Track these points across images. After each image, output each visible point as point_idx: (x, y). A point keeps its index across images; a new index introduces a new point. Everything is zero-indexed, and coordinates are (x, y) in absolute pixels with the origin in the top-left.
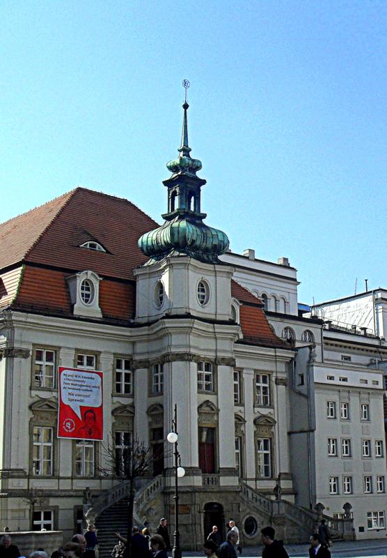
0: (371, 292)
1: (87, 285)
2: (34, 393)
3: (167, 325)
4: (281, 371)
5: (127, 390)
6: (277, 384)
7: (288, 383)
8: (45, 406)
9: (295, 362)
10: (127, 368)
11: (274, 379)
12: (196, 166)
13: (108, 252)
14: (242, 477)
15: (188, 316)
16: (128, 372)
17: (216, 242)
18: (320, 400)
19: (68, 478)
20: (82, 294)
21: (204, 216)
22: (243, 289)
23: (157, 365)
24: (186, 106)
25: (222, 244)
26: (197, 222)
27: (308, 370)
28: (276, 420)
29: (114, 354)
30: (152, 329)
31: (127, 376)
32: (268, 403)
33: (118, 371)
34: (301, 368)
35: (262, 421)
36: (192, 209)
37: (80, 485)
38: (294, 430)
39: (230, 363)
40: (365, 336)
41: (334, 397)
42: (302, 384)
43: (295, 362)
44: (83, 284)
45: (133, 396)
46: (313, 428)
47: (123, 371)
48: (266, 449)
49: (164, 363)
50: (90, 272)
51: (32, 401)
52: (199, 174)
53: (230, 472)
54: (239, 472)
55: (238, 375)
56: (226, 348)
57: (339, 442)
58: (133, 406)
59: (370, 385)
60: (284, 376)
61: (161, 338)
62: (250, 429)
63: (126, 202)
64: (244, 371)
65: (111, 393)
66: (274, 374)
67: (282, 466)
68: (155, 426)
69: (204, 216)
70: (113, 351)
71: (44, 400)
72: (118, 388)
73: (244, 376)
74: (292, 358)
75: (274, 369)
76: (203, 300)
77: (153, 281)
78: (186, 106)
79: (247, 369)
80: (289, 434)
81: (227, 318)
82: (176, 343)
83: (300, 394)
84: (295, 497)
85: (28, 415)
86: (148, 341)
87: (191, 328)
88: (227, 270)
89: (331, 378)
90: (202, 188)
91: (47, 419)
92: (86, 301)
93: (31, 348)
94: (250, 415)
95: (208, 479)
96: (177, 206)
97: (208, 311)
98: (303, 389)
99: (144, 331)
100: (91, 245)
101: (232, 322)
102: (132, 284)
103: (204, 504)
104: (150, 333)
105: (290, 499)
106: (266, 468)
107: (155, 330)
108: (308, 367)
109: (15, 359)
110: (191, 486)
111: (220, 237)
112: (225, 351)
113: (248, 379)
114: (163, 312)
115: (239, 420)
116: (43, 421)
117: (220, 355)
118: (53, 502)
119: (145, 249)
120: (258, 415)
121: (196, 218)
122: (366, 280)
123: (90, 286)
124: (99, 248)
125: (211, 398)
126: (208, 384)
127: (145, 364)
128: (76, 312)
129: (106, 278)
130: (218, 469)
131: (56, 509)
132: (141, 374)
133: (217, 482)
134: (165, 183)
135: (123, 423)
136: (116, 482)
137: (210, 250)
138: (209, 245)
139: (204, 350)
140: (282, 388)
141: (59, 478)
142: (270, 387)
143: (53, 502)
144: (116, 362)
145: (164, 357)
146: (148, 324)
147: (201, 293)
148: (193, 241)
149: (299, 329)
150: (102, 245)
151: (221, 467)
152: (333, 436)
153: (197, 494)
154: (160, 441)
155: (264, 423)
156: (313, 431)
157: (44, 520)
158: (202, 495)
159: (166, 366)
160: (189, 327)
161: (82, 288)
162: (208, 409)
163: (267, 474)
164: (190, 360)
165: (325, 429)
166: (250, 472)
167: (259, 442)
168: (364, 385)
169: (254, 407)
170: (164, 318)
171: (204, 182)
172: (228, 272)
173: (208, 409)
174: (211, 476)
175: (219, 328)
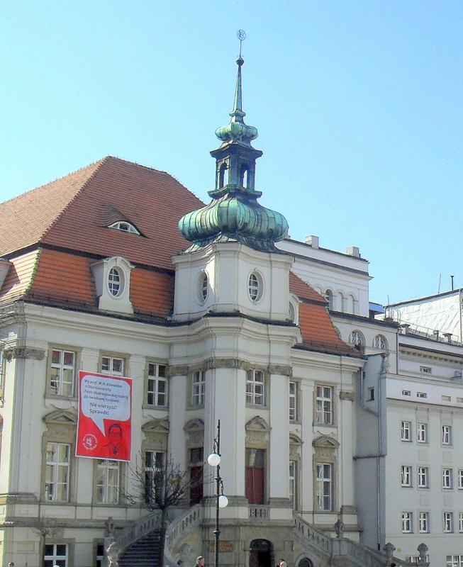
1: (116, 274)
2: (49, 402)
3: (211, 325)
4: (346, 382)
5: (161, 401)
8: (62, 418)
9: (364, 373)
10: (161, 374)
13: (142, 235)
14: (296, 509)
15: (237, 314)
16: (162, 379)
17: (272, 226)
18: (393, 419)
19: (87, 506)
20: (110, 284)
21: (260, 194)
22: (304, 283)
23: (199, 373)
24: (240, 62)
25: (280, 230)
26: (250, 201)
28: (339, 441)
29: (146, 357)
30: (193, 329)
31: (162, 385)
32: (330, 420)
33: (151, 378)
34: (371, 381)
35: (322, 443)
36: (245, 185)
37: (102, 514)
38: (361, 455)
39: (286, 372)
40: (450, 343)
41: (410, 416)
42: (373, 399)
43: (364, 373)
44: (111, 272)
45: (168, 409)
46: (384, 454)
47: (157, 378)
48: (326, 476)
49: (206, 370)
50: (120, 258)
51: (46, 411)
52: (255, 144)
53: (283, 503)
54: (293, 502)
55: (294, 386)
56: (281, 353)
57: (415, 470)
58: (167, 421)
60: (349, 389)
61: (203, 340)
62: (307, 452)
63: (165, 177)
64: (303, 382)
65: (141, 404)
66: (339, 387)
67: (345, 495)
68: (194, 446)
69: (260, 194)
70: (145, 355)
71: (61, 410)
72: (150, 400)
74: (360, 368)
75: (338, 380)
78: (240, 62)
79: (305, 379)
80: (355, 459)
81: (283, 318)
82: (222, 346)
83: (369, 411)
84: (360, 535)
86: (188, 343)
87: (240, 329)
88: (285, 260)
89: (407, 393)
90: (257, 160)
91: (63, 434)
92: (115, 293)
93: (46, 347)
94: (308, 434)
95: (256, 510)
96: (226, 182)
97: (261, 309)
98: (373, 405)
99: (183, 330)
100: (122, 226)
101: (289, 323)
102: (172, 274)
103: (250, 541)
104: (190, 333)
105: (354, 537)
106: (326, 500)
107: (197, 330)
108: (380, 379)
110: (235, 519)
111: (278, 221)
112: (279, 357)
113: (307, 392)
114: (207, 308)
115: (295, 441)
117: (274, 362)
118: (68, 534)
119: (187, 233)
120: (319, 435)
121: (248, 197)
122: (452, 277)
123: (119, 276)
124: (131, 230)
125: (262, 413)
126: (259, 396)
127: (184, 371)
129: (139, 266)
130: (268, 500)
131: (72, 542)
132: (179, 385)
133: (266, 514)
134: (214, 154)
135: (154, 441)
136: (145, 512)
137: (265, 237)
138: (264, 230)
139: (256, 355)
141: (76, 505)
142: (333, 402)
143: (68, 534)
144: (148, 368)
145: (207, 362)
146: (189, 323)
147: (254, 288)
148: (246, 224)
149: (370, 333)
150: (135, 227)
151: (271, 496)
152: (407, 464)
154: (199, 464)
155: (325, 445)
156: (383, 456)
157: (58, 554)
159: (208, 373)
160: (237, 328)
161: (110, 278)
162: (257, 426)
163: (326, 507)
164: (238, 368)
165: (398, 453)
166: (307, 502)
167: (318, 468)
168: (447, 403)
169: (313, 425)
170: (207, 315)
171: (259, 154)
172: (286, 263)
173: (257, 426)
174: (259, 507)
175: (274, 330)
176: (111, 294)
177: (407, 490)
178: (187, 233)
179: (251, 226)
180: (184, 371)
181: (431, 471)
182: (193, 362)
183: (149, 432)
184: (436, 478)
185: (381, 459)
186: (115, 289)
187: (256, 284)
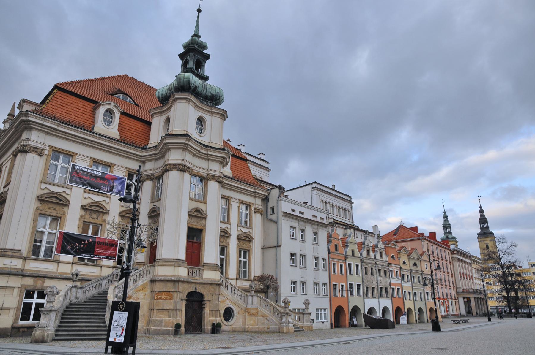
0: (308, 184)
1: (110, 112)
2: (44, 186)
6: (255, 212)
7: (263, 213)
9: (268, 199)
11: (253, 209)
13: (136, 104)
14: (226, 276)
17: (213, 92)
18: (285, 225)
19: (68, 263)
20: (105, 120)
23: (158, 178)
24: (199, 11)
27: (278, 203)
28: (253, 237)
29: (127, 168)
32: (248, 223)
34: (272, 203)
41: (295, 224)
42: (273, 212)
48: (245, 257)
50: (112, 104)
53: (211, 267)
57: (298, 256)
59: (318, 220)
61: (163, 156)
64: (232, 200)
66: (254, 206)
71: (53, 193)
73: (232, 203)
74: (266, 196)
75: (253, 202)
76: (201, 131)
77: (164, 117)
78: (199, 11)
80: (264, 248)
83: (271, 220)
85: (34, 204)
87: (188, 145)
89: (293, 211)
91: (55, 209)
93: (47, 148)
97: (205, 139)
98: (274, 217)
103: (187, 292)
106: (245, 272)
108: (278, 201)
109: (28, 154)
110: (175, 276)
116: (50, 210)
119: (160, 97)
120: (240, 232)
125: (201, 206)
127: (151, 178)
128: (95, 130)
132: (147, 186)
133: (201, 275)
138: (208, 94)
140: (258, 216)
150: (131, 98)
151: (205, 262)
153: (180, 283)
156: (278, 246)
157: (37, 298)
158: (185, 285)
160: (185, 144)
162: (197, 214)
163: (244, 276)
164: (184, 171)
165: (288, 246)
168: (314, 219)
172: (221, 114)
173: (197, 214)
174: (195, 268)
176: (106, 126)
177: (294, 268)
178: (160, 97)
179: (199, 89)
180: (151, 178)
181: (307, 257)
183: (124, 216)
184: (310, 261)
185: (278, 248)
186: (109, 123)
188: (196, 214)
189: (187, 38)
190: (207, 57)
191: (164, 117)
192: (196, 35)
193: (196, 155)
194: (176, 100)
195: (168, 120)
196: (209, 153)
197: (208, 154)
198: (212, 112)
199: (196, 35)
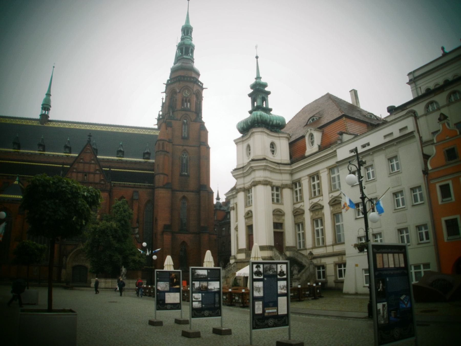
12: (265, 85)
23: (247, 190)
24: (257, 57)
52: (267, 89)
76: (273, 152)
78: (257, 57)
126: (277, 199)
146: (243, 167)
159: (253, 188)
170: (250, 161)
173: (278, 214)
175: (282, 168)
182: (247, 186)
187: (273, 148)
188: (278, 213)
189: (253, 81)
190: (269, 93)
191: (245, 145)
192: (258, 78)
193: (273, 171)
194: (254, 132)
195: (249, 146)
196: (281, 168)
197: (280, 170)
198: (279, 137)
199: (258, 78)
